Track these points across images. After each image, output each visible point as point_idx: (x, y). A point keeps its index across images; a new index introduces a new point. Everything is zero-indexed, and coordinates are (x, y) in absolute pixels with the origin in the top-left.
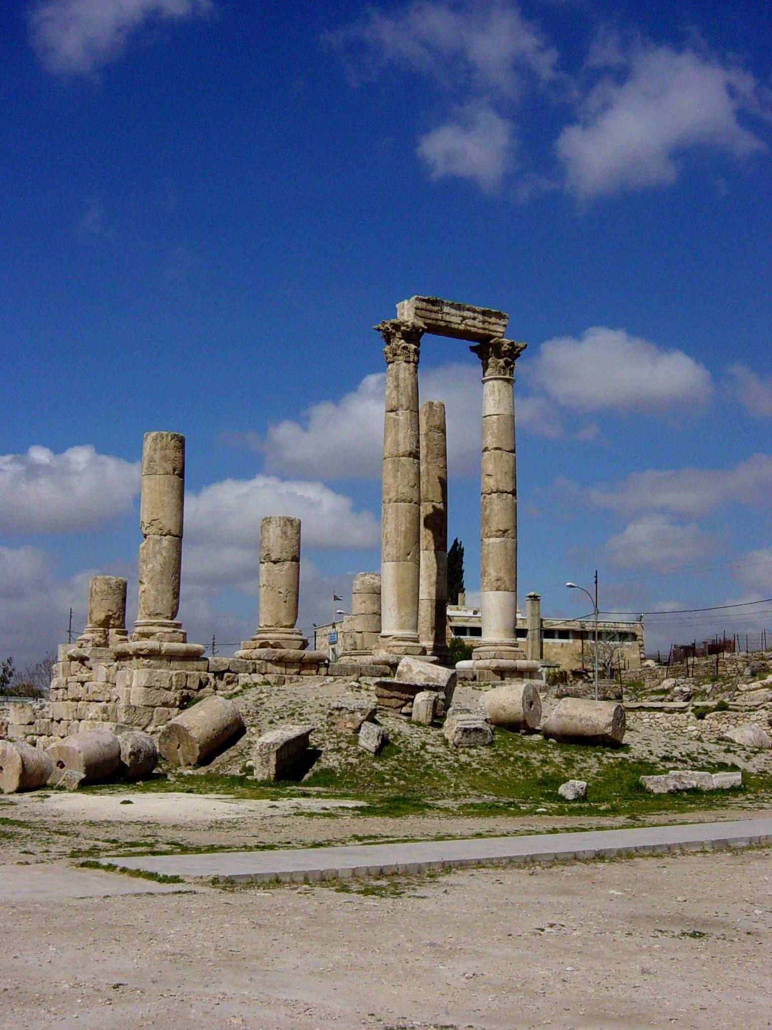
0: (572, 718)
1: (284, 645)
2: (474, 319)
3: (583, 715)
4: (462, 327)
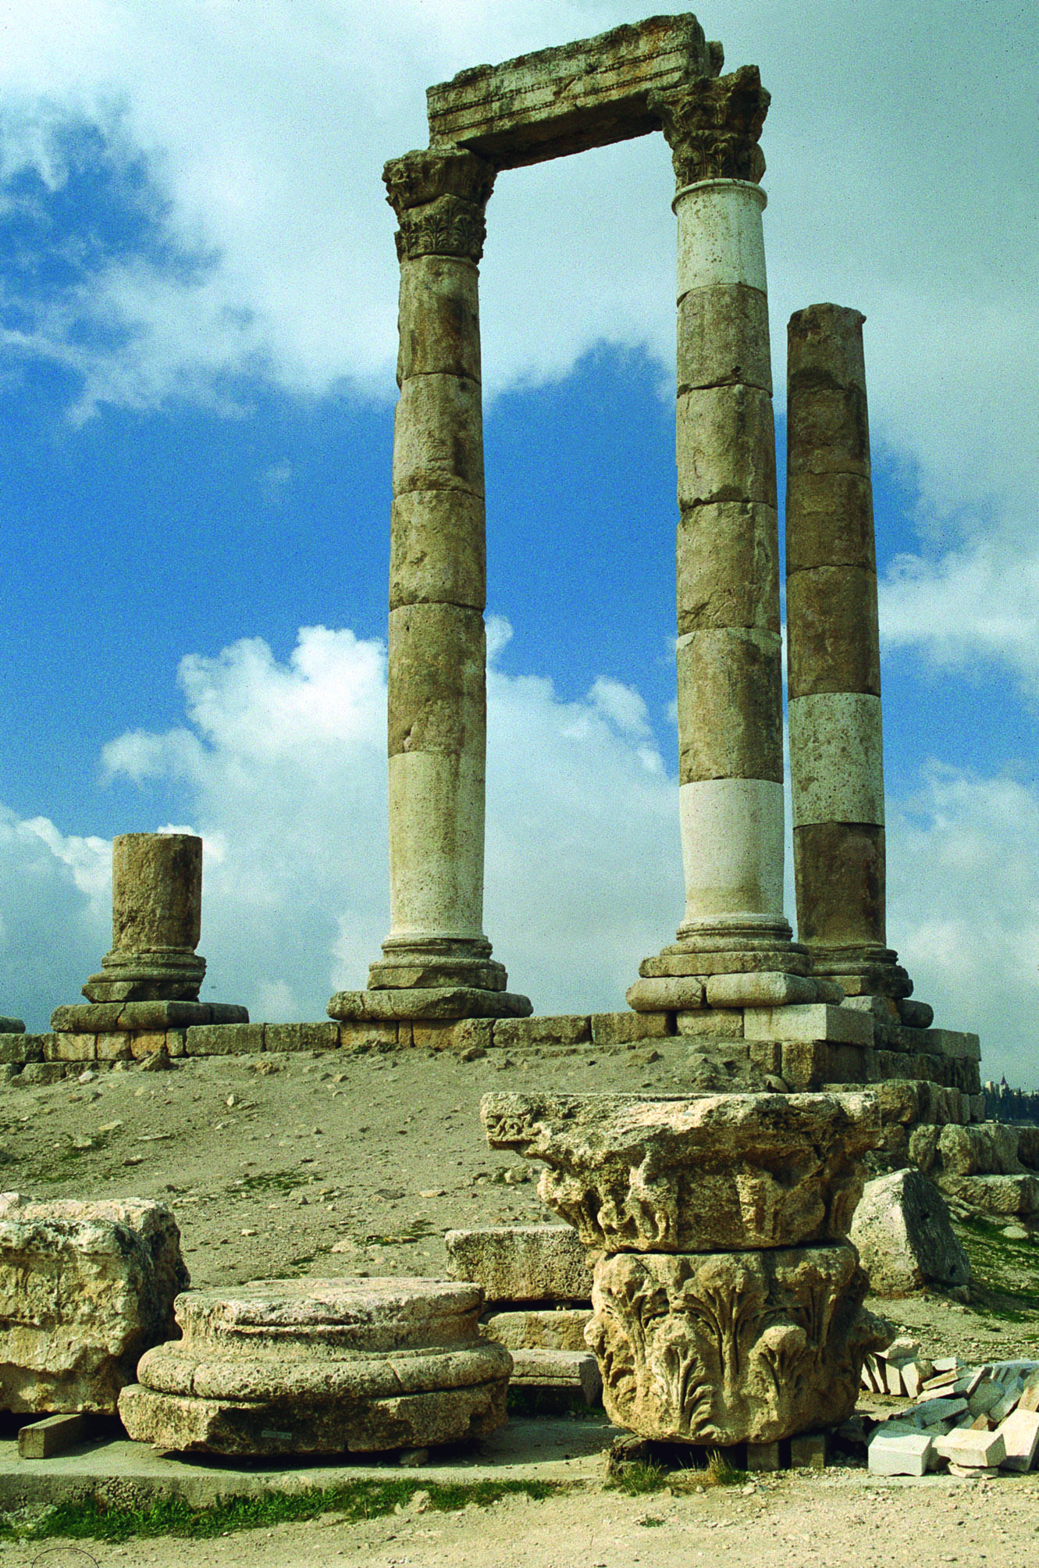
2: (591, 69)
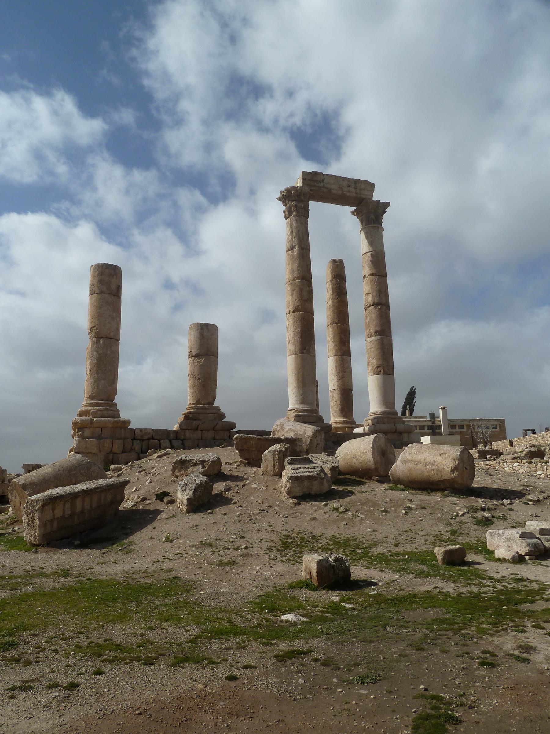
0: (417, 463)
2: (349, 186)
3: (427, 460)
4: (340, 192)
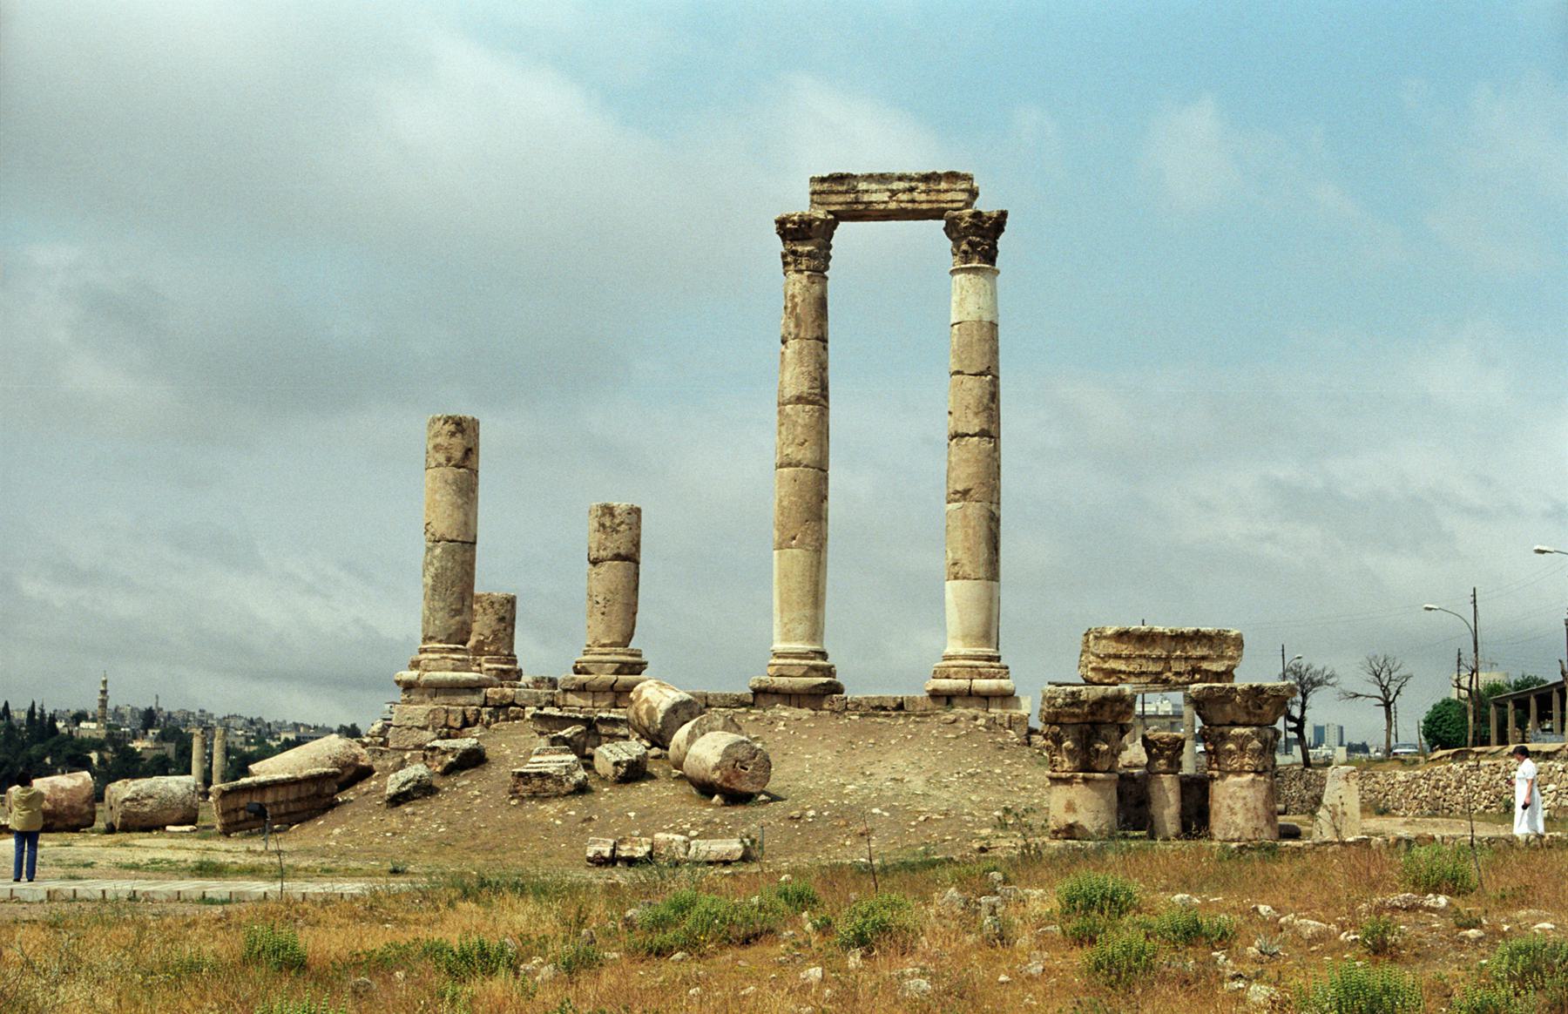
1: (592, 669)
2: (912, 190)
